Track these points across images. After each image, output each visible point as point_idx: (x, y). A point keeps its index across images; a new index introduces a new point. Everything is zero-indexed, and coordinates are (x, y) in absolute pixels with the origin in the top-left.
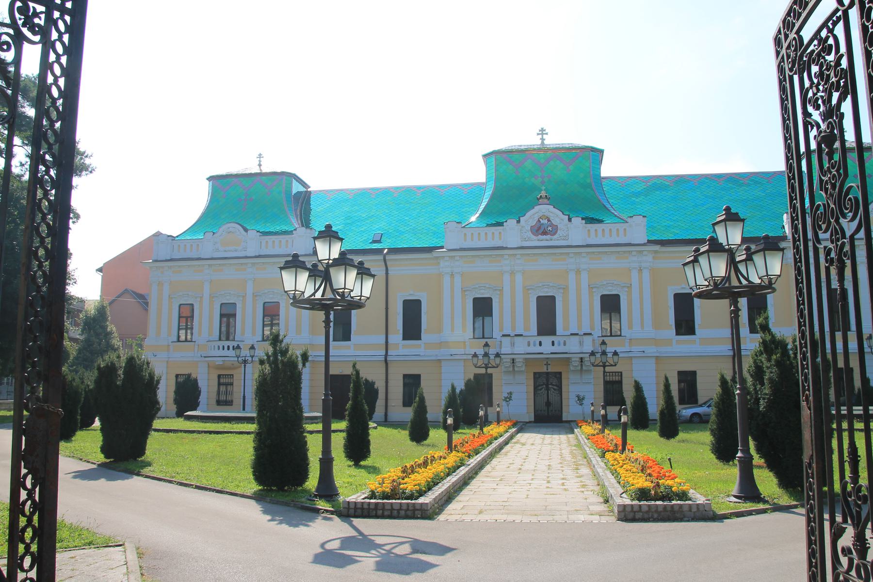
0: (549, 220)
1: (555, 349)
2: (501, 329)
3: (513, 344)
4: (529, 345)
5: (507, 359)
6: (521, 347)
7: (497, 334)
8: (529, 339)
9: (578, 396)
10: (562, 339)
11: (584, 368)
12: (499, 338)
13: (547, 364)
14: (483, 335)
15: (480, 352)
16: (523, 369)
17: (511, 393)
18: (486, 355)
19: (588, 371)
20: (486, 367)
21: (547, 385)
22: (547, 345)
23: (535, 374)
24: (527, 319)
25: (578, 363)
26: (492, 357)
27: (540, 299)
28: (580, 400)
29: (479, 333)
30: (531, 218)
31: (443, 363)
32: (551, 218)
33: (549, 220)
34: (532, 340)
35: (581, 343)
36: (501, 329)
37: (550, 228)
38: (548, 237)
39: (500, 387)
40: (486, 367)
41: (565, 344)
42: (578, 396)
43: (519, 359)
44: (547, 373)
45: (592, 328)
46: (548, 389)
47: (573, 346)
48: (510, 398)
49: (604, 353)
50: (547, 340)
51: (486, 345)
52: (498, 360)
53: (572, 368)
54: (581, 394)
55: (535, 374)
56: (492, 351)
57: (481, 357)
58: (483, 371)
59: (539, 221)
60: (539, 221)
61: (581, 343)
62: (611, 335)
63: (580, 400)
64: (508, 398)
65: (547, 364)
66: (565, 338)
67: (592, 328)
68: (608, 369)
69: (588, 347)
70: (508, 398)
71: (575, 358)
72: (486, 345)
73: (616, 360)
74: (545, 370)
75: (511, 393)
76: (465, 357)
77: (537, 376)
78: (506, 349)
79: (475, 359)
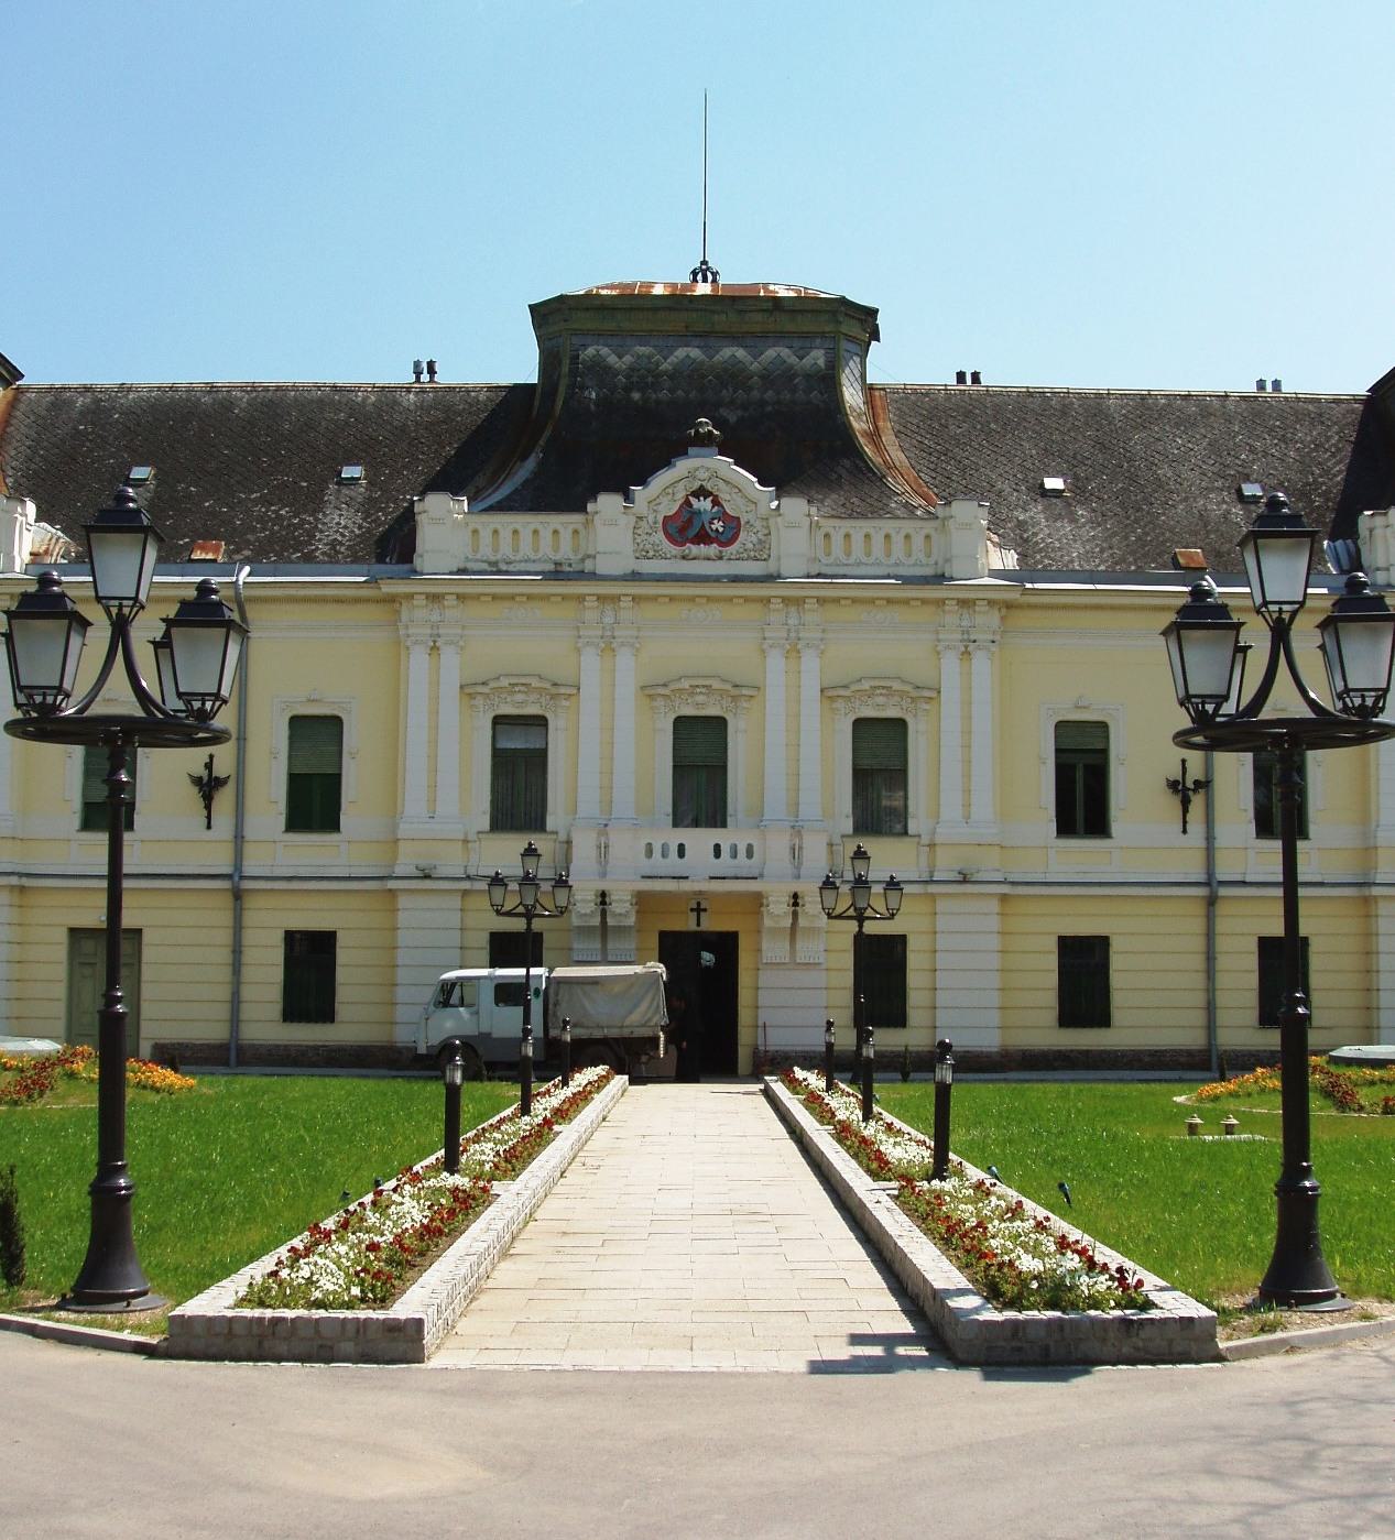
0: (716, 502)
11: (802, 922)
13: (699, 910)
16: (631, 921)
20: (529, 915)
27: (684, 727)
30: (664, 490)
32: (723, 497)
33: (716, 502)
37: (718, 525)
38: (713, 549)
49: (861, 883)
50: (700, 840)
53: (767, 922)
58: (518, 925)
59: (687, 503)
60: (687, 503)
68: (871, 928)
73: (893, 904)
79: (498, 892)
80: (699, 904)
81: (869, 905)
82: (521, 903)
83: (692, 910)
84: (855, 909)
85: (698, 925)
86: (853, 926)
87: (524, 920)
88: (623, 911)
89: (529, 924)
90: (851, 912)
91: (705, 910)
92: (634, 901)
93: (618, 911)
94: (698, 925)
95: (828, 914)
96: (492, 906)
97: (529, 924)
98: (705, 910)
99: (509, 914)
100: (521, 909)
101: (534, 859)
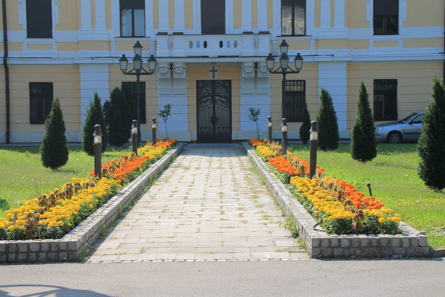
11: (259, 75)
13: (214, 71)
16: (184, 76)
20: (138, 74)
49: (284, 57)
53: (244, 75)
58: (133, 78)
68: (289, 77)
73: (299, 66)
79: (124, 64)
80: (214, 68)
81: (288, 66)
82: (134, 69)
83: (211, 71)
84: (282, 69)
85: (214, 77)
86: (281, 76)
87: (136, 76)
88: (180, 72)
89: (138, 78)
90: (280, 70)
91: (216, 71)
92: (185, 67)
93: (178, 72)
94: (214, 77)
95: (270, 71)
96: (121, 70)
97: (138, 78)
98: (216, 71)
99: (129, 73)
100: (134, 71)
101: (140, 49)
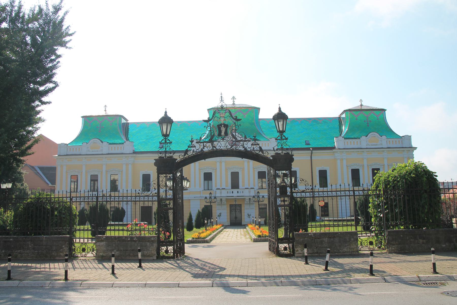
1: (239, 195)
2: (216, 186)
3: (221, 193)
4: (228, 193)
5: (218, 199)
6: (224, 194)
7: (214, 188)
8: (227, 190)
9: (248, 214)
10: (242, 190)
12: (215, 190)
13: (235, 201)
14: (208, 188)
15: (208, 196)
17: (220, 213)
18: (210, 198)
19: (253, 204)
20: (211, 203)
21: (235, 210)
22: (235, 193)
23: (230, 205)
24: (227, 181)
25: (248, 200)
26: (213, 198)
27: (232, 173)
28: (249, 216)
29: (206, 188)
31: (191, 201)
34: (229, 191)
35: (249, 192)
36: (216, 186)
39: (216, 211)
40: (211, 203)
41: (243, 192)
42: (248, 214)
43: (223, 199)
44: (236, 205)
45: (254, 185)
46: (236, 212)
47: (246, 193)
48: (220, 215)
50: (235, 191)
51: (211, 193)
52: (215, 200)
54: (250, 213)
55: (230, 205)
56: (213, 195)
57: (208, 198)
58: (209, 204)
61: (249, 192)
62: (262, 189)
63: (249, 216)
64: (220, 215)
65: (235, 201)
66: (242, 190)
67: (254, 185)
69: (253, 193)
70: (220, 215)
71: (247, 198)
72: (211, 193)
74: (235, 203)
75: (220, 213)
76: (200, 198)
77: (231, 206)
78: (218, 195)
79: (206, 199)
